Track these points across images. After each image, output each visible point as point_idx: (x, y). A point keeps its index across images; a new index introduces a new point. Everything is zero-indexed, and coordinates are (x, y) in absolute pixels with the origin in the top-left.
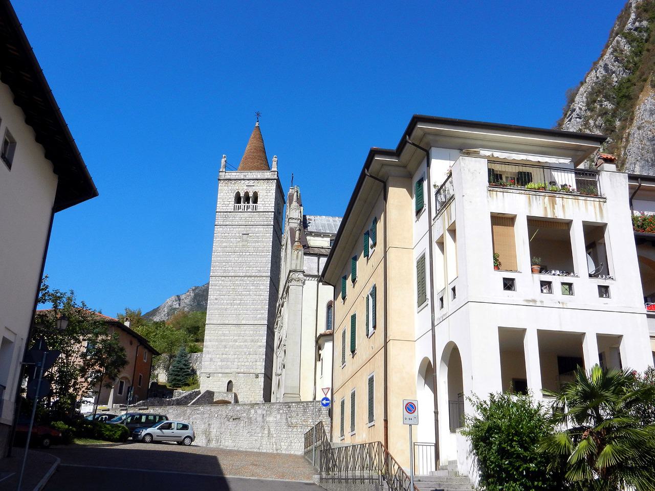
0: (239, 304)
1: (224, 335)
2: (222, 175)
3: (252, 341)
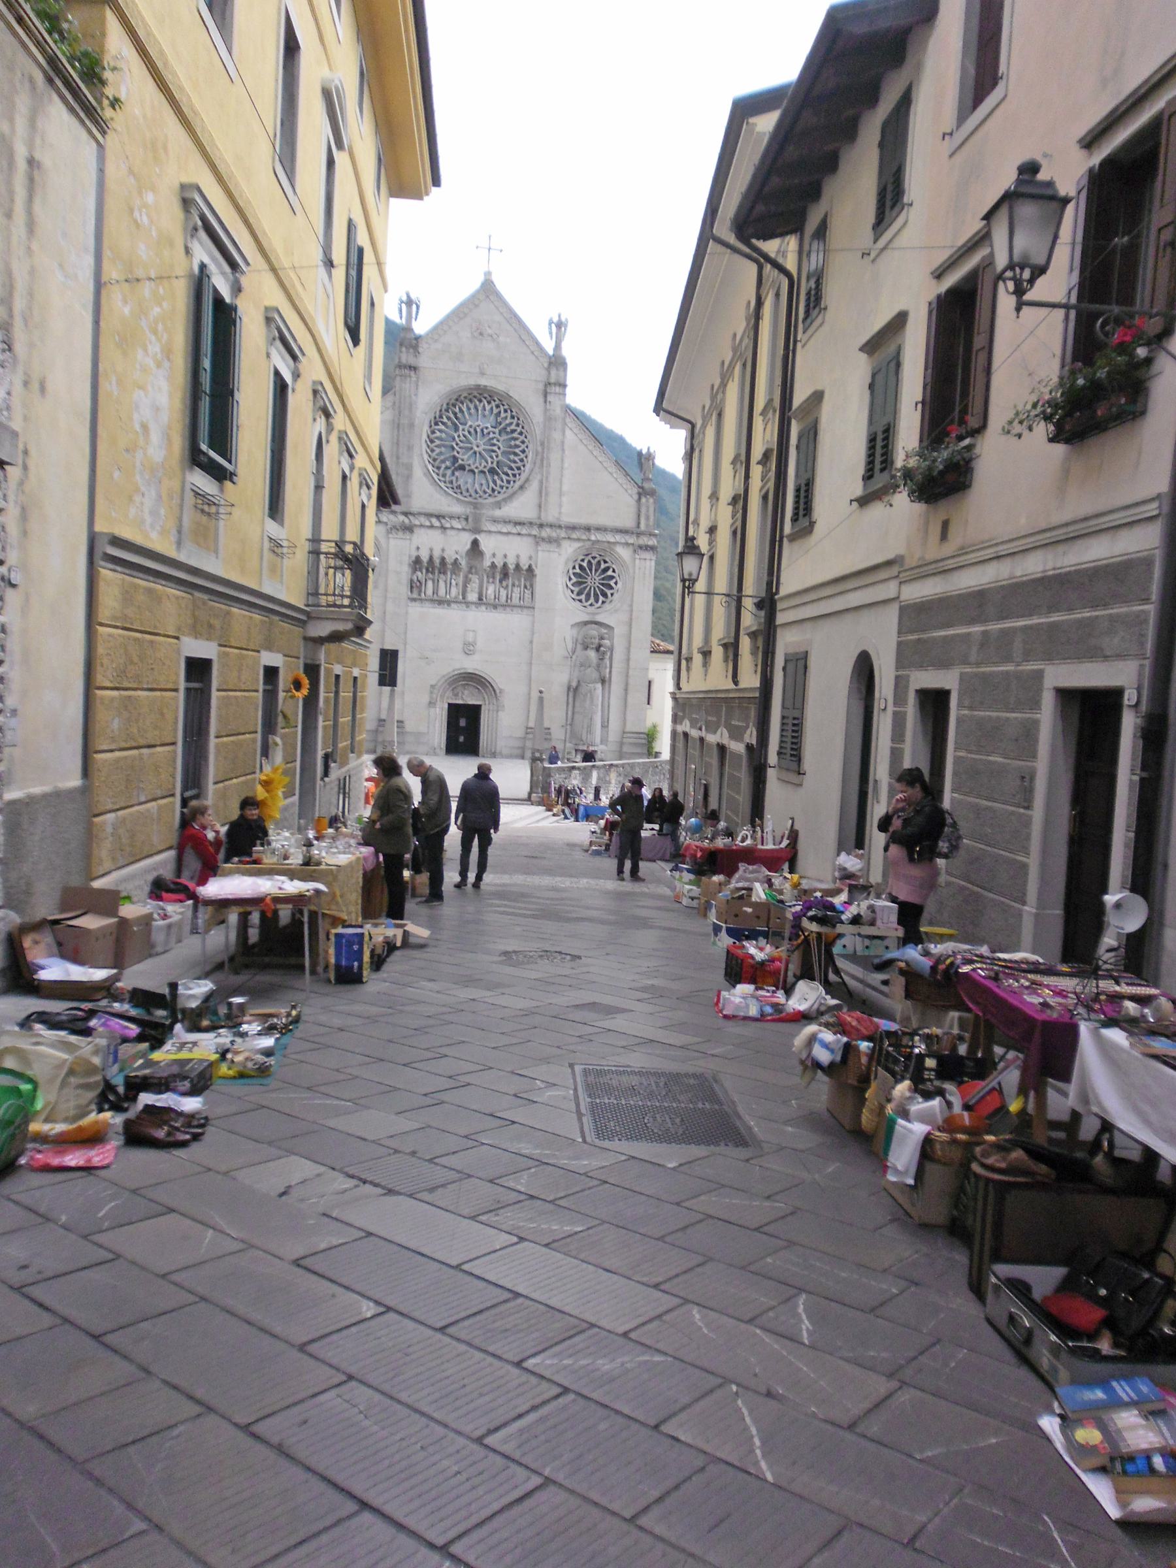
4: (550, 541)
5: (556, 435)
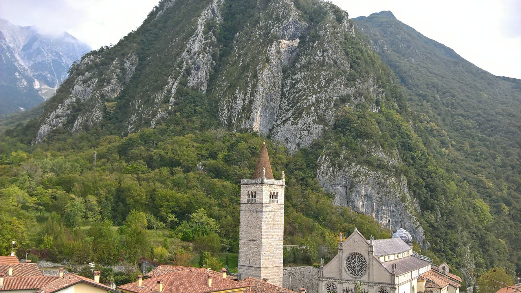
0: (273, 256)
1: (268, 273)
2: (266, 181)
3: (278, 275)
4: (371, 286)
5: (371, 263)
